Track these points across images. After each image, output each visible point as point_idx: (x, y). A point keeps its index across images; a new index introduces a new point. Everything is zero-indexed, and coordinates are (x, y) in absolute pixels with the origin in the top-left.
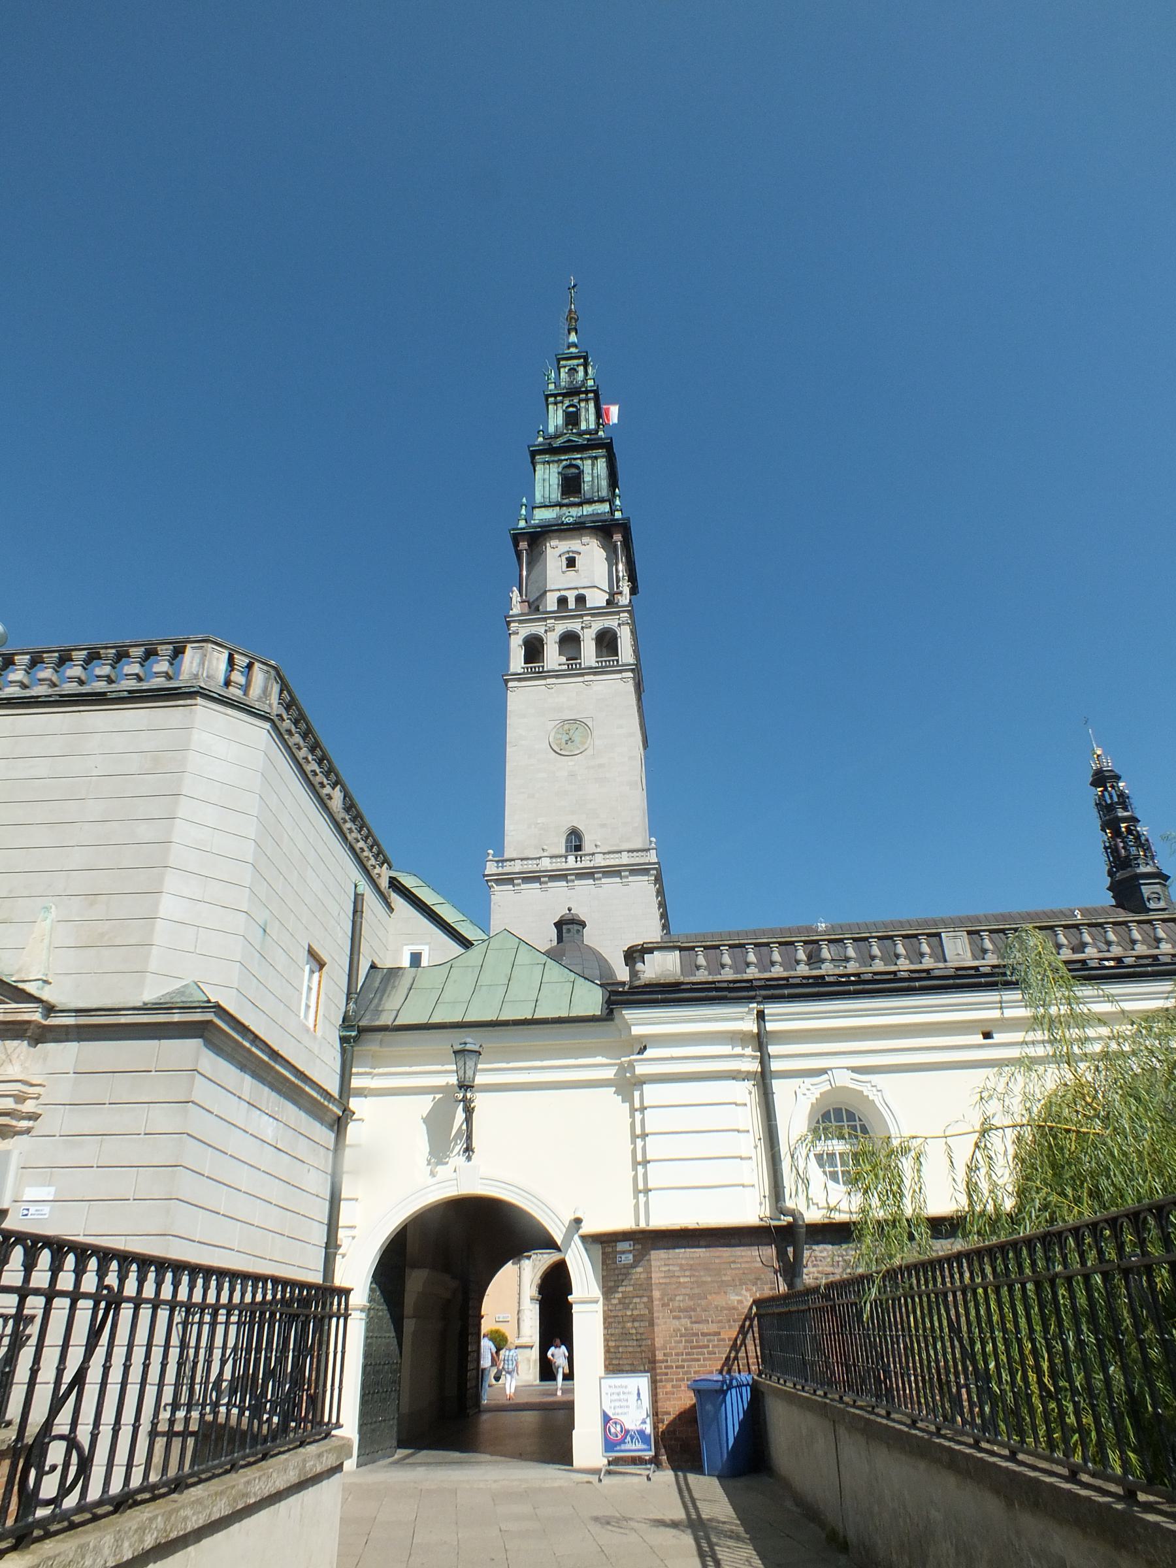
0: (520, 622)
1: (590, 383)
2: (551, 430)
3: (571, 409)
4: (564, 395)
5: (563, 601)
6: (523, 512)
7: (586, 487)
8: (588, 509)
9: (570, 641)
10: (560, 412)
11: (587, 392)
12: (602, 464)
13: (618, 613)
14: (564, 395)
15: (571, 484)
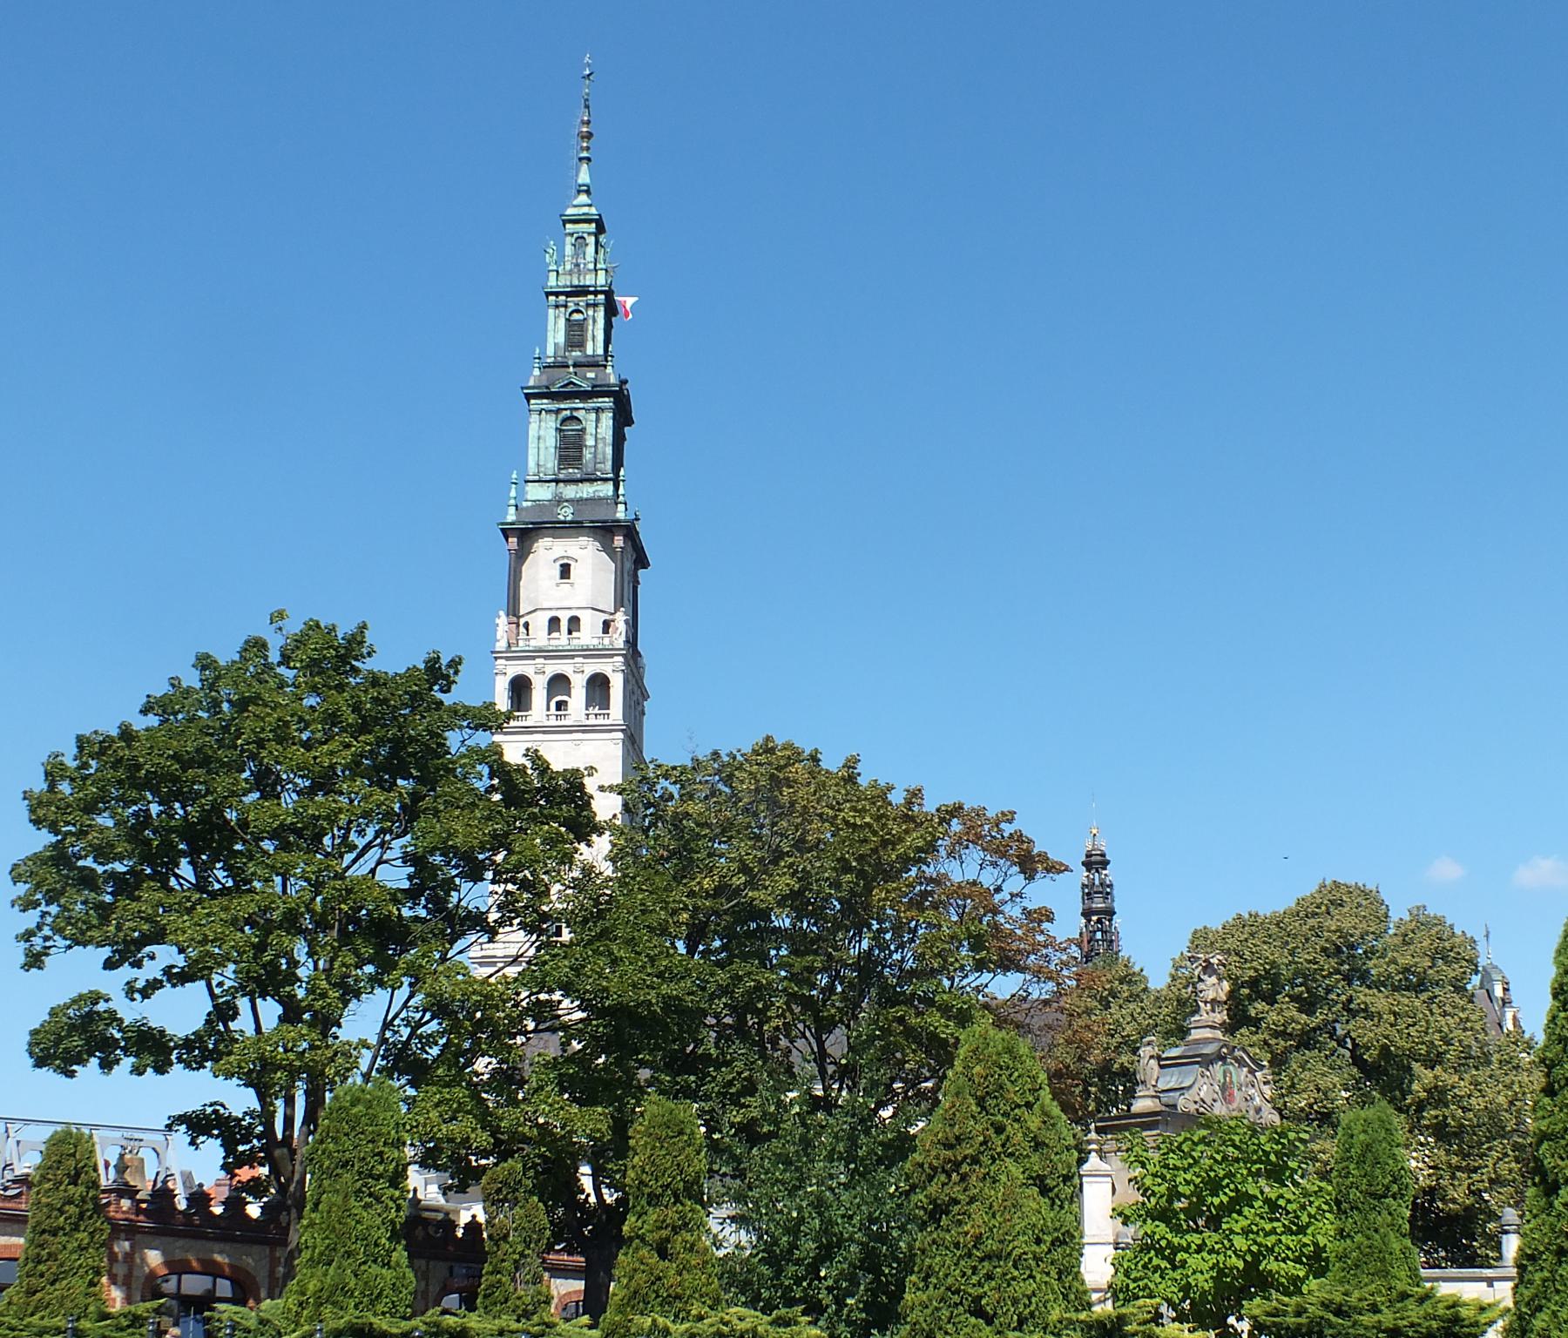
0: (507, 659)
1: (602, 279)
2: (550, 351)
3: (576, 316)
4: (568, 294)
5: (554, 623)
6: (513, 494)
7: (587, 455)
8: (586, 490)
9: (559, 683)
10: (562, 323)
11: (596, 293)
12: (607, 420)
13: (612, 656)
14: (568, 294)
15: (570, 449)
